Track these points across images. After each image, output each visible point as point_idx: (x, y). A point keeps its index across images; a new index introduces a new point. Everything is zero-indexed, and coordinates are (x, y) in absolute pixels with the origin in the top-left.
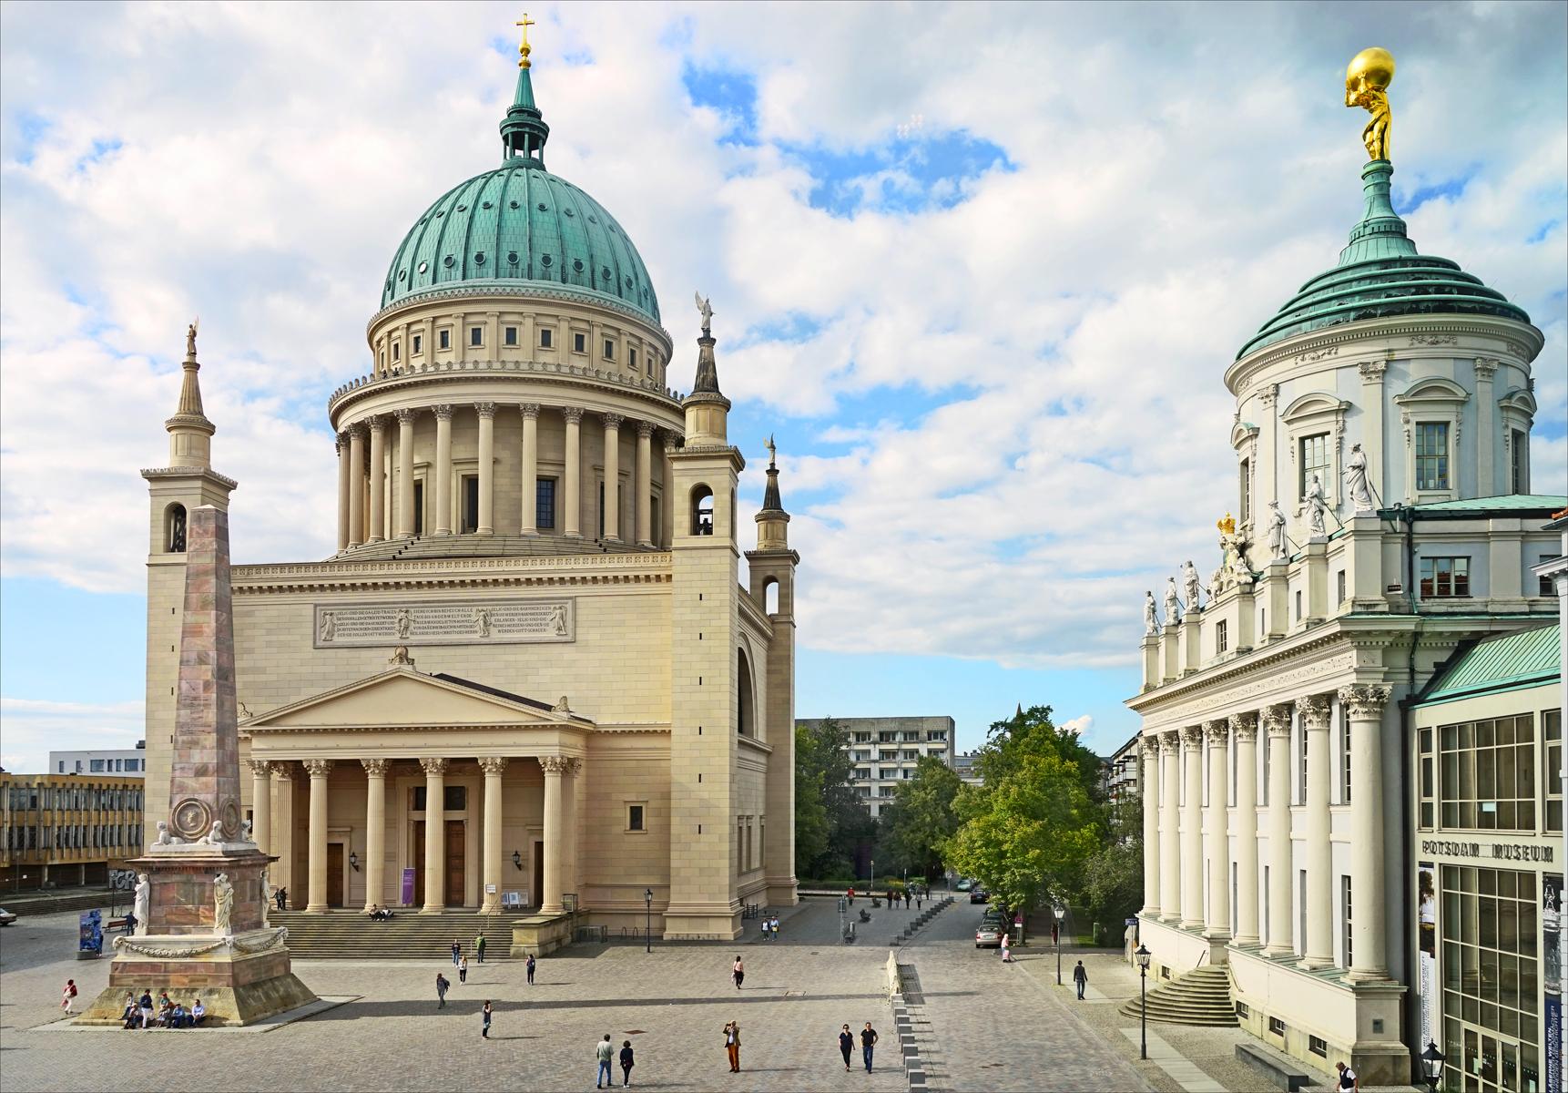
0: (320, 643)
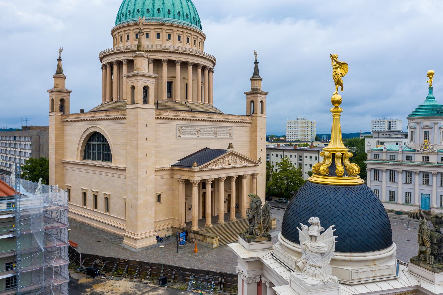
0: (178, 138)
